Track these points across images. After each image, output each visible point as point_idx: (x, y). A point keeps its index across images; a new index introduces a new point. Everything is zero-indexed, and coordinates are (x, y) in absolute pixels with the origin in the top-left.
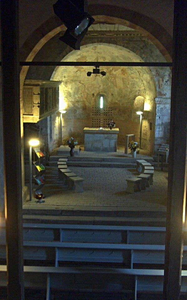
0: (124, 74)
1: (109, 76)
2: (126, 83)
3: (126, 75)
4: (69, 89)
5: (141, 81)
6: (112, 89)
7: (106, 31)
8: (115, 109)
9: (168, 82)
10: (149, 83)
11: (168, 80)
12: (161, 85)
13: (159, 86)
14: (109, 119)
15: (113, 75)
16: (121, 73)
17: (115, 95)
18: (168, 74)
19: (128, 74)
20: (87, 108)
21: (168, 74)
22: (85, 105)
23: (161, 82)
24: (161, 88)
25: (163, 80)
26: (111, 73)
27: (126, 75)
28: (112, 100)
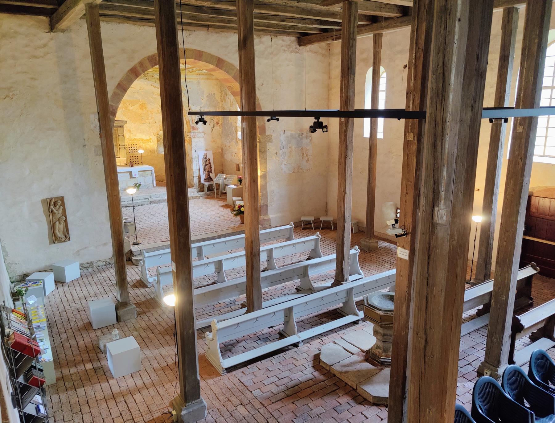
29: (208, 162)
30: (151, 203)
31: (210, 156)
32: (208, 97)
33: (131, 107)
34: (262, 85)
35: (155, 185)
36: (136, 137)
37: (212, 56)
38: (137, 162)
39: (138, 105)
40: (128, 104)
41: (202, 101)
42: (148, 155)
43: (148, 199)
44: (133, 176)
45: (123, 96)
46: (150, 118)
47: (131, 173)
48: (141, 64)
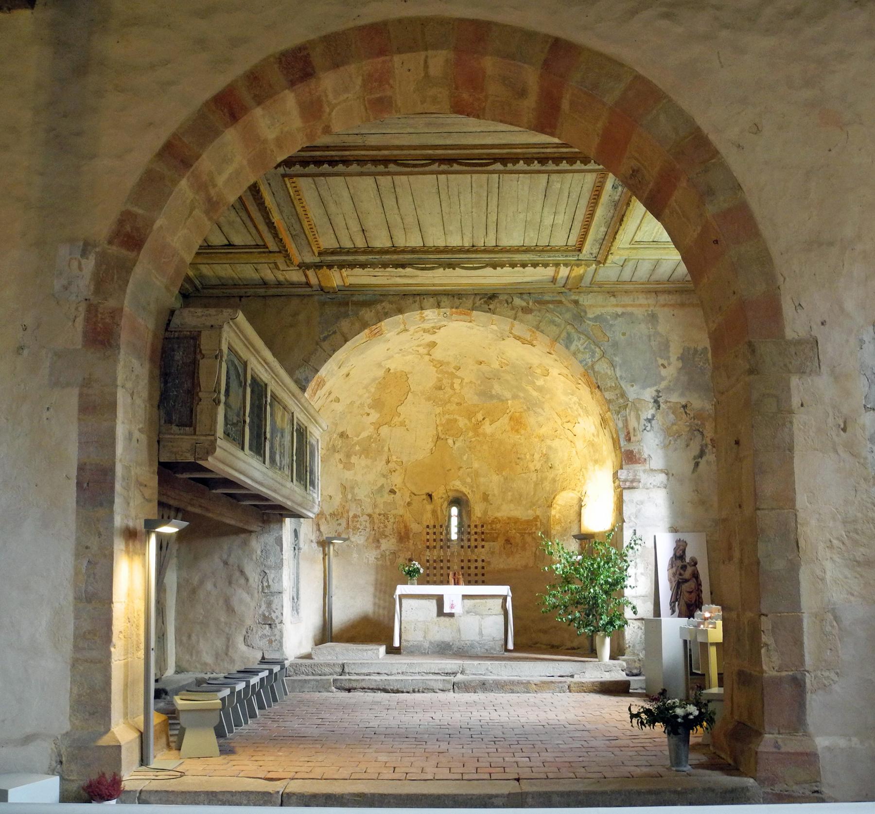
0: (517, 431)
1: (473, 439)
2: (523, 456)
3: (523, 432)
4: (355, 474)
5: (569, 443)
6: (482, 480)
7: (461, 250)
8: (494, 540)
9: (653, 422)
10: (592, 444)
11: (653, 416)
12: (634, 429)
13: (628, 433)
14: (476, 547)
15: (485, 435)
16: (508, 428)
17: (494, 495)
18: (653, 398)
19: (529, 428)
20: (411, 535)
21: (653, 398)
22: (405, 527)
23: (633, 423)
24: (633, 439)
25: (638, 418)
26: (481, 431)
27: (523, 432)
28: (485, 512)
29: (690, 570)
30: (456, 687)
31: (695, 550)
32: (681, 358)
33: (488, 428)
34: (757, 129)
35: (511, 646)
36: (499, 515)
37: (529, 36)
38: (480, 578)
39: (504, 421)
40: (480, 417)
41: (664, 372)
42: (526, 567)
43: (455, 674)
44: (447, 610)
45: (175, 182)
46: (537, 456)
47: (440, 600)
48: (253, 78)
